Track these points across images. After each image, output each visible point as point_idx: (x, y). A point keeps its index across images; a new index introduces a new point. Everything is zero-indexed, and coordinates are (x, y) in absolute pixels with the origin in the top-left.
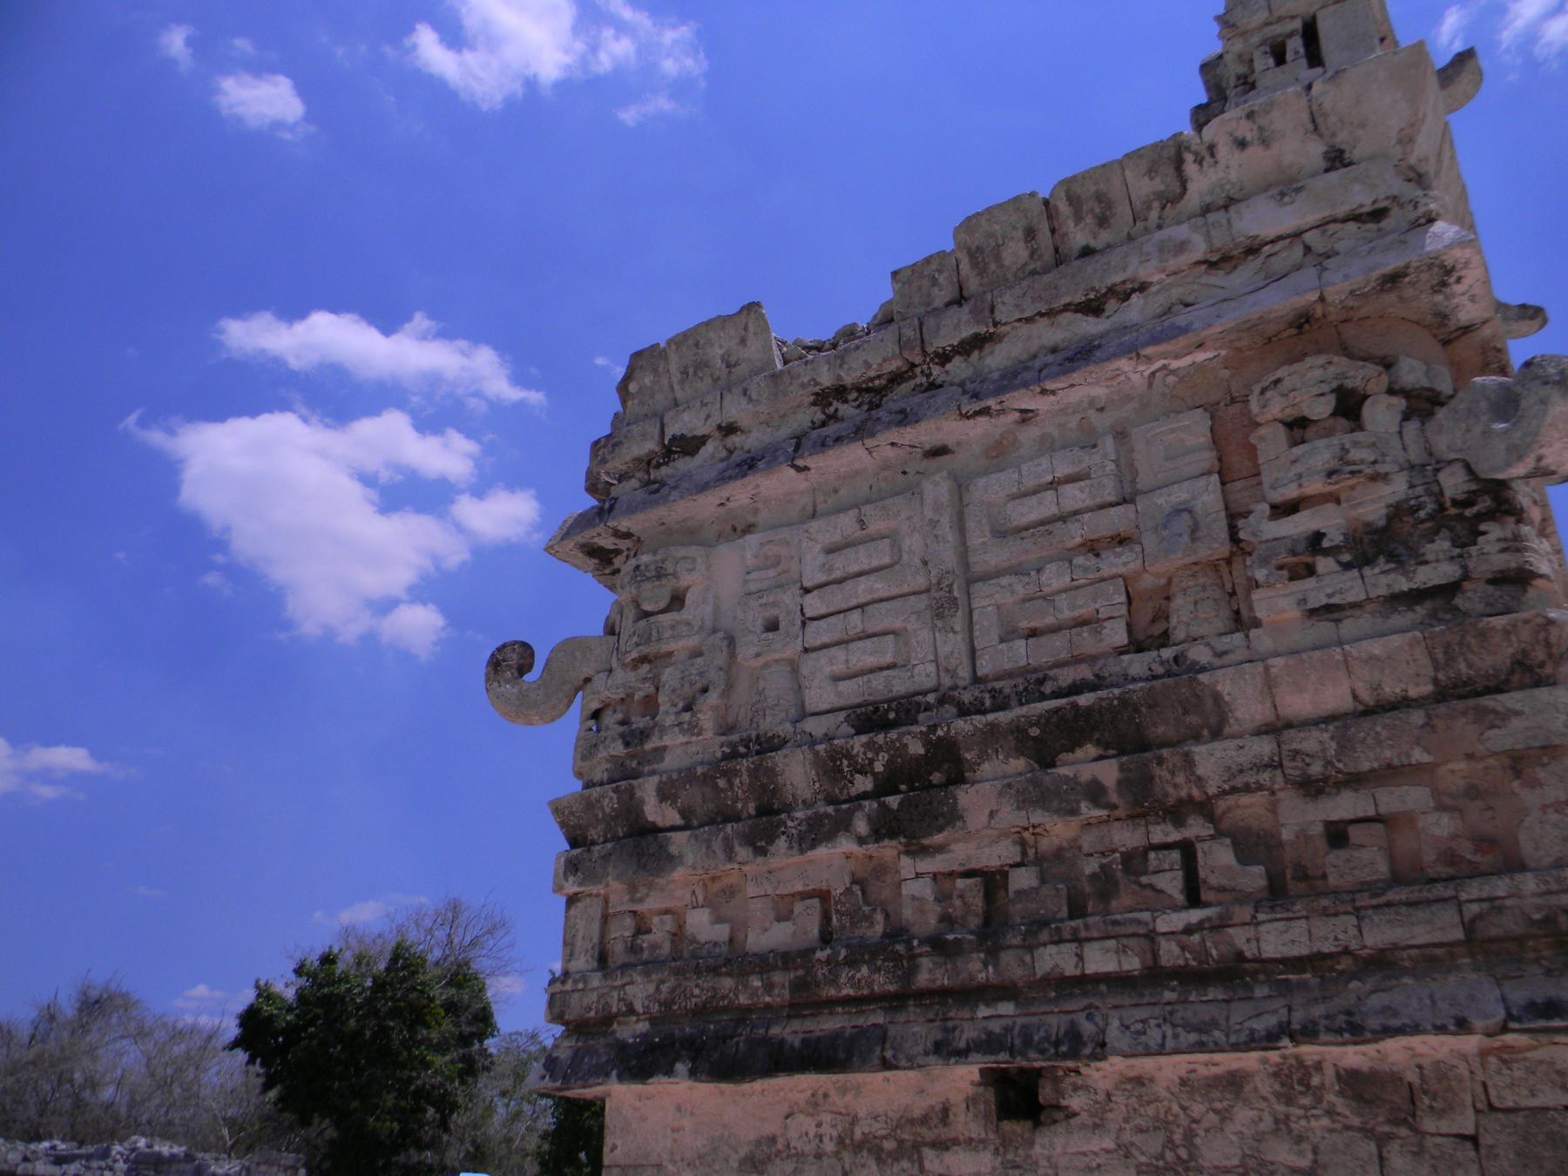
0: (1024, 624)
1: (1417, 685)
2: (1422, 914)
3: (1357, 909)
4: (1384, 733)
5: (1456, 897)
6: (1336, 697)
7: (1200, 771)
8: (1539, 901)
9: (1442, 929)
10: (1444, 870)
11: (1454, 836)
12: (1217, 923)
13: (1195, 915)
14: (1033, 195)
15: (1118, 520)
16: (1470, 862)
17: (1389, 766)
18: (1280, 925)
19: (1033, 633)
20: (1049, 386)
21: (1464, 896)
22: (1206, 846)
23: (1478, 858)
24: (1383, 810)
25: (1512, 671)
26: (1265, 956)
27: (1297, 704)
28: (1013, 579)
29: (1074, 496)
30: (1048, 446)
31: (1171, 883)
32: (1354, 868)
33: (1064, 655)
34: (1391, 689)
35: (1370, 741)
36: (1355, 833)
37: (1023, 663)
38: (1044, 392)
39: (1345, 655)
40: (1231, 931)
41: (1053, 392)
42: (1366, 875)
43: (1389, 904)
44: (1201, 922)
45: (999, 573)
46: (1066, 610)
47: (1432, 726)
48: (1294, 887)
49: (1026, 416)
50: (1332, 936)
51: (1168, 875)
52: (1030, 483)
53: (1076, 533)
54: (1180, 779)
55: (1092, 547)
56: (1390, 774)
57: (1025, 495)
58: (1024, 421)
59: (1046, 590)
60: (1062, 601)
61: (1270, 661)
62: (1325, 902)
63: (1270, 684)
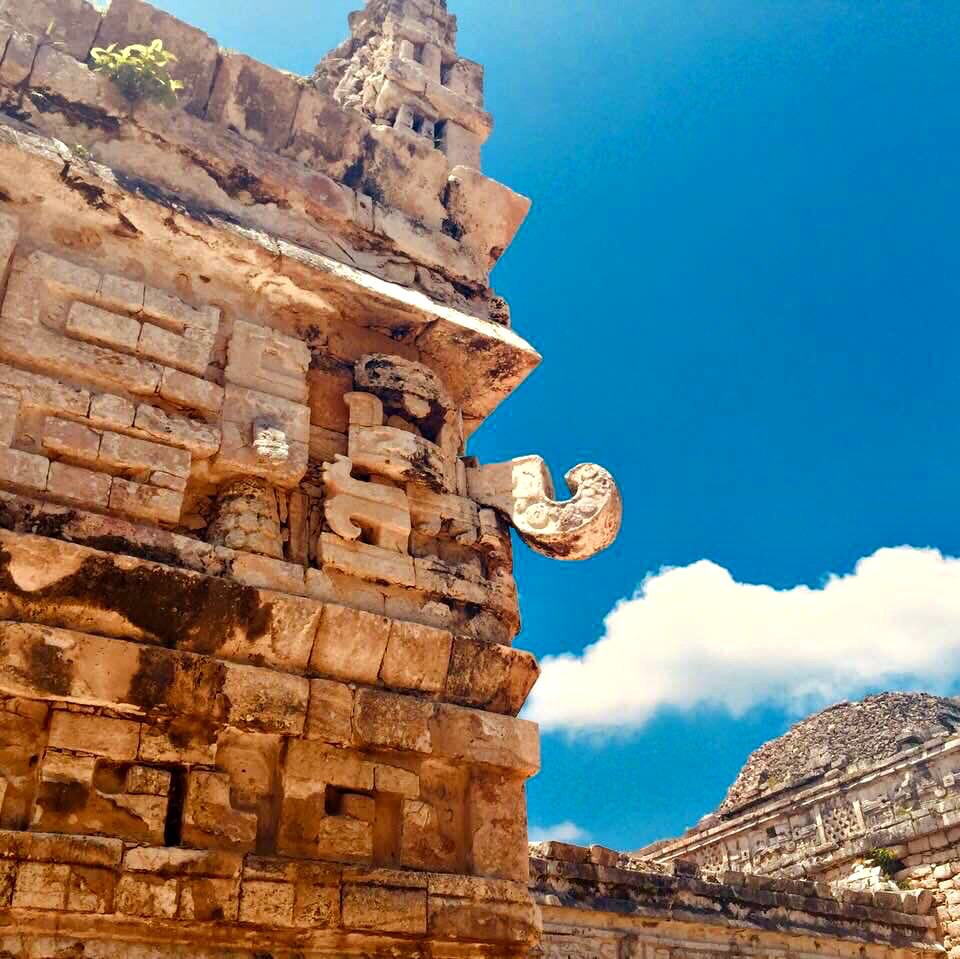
0: (56, 444)
1: (432, 680)
2: (399, 900)
3: (343, 884)
4: (401, 713)
5: (426, 889)
6: (365, 663)
7: (228, 690)
8: (484, 906)
9: (411, 919)
10: (417, 861)
11: (428, 829)
12: (201, 869)
13: (177, 856)
14: (212, 42)
15: (201, 392)
16: (436, 857)
17: (398, 747)
18: (267, 887)
19: (55, 457)
20: (179, 220)
21: (432, 890)
22: (203, 776)
23: (442, 855)
24: (380, 786)
25: (496, 695)
26: (244, 919)
27: (336, 656)
28: (56, 388)
29: (158, 341)
30: (134, 271)
31: (151, 812)
32: (345, 839)
33: (98, 500)
34: (410, 676)
35: (389, 716)
36: (351, 802)
37: (41, 485)
38: (169, 222)
39: (393, 629)
40: (215, 882)
41: (176, 230)
42: (351, 848)
43: (371, 884)
44: (184, 865)
45: (33, 368)
46: (115, 451)
47: (439, 721)
48: (284, 844)
49: (125, 229)
50: (315, 908)
51: (152, 801)
52: (109, 299)
53: (147, 381)
54: (204, 692)
55: (158, 400)
56: (403, 756)
57: (98, 305)
58: (117, 233)
59: (95, 419)
60: (113, 441)
61: (328, 606)
62: (316, 870)
63: (319, 628)
